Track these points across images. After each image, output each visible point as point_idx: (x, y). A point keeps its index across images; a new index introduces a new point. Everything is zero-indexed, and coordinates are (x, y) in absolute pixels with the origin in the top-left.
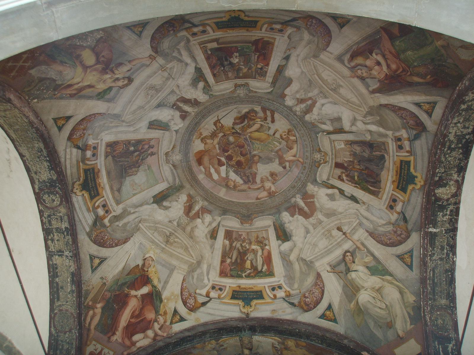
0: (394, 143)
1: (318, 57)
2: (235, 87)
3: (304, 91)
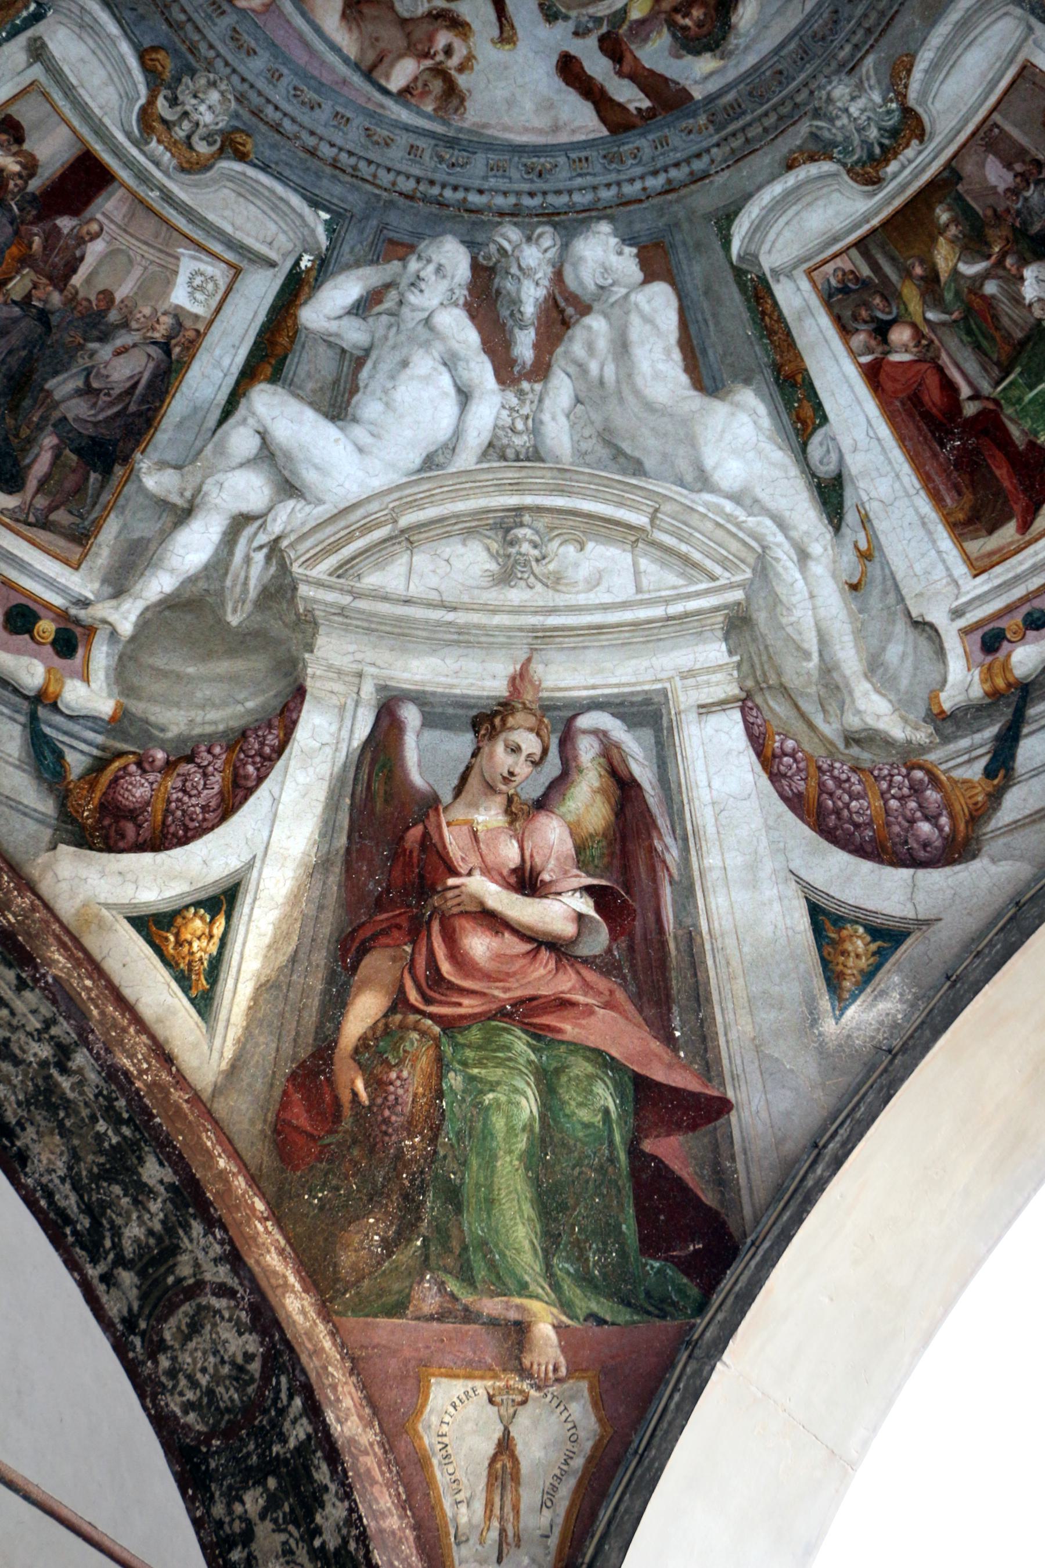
0: (57, 601)
1: (726, 639)
2: (907, 112)
3: (601, 383)
